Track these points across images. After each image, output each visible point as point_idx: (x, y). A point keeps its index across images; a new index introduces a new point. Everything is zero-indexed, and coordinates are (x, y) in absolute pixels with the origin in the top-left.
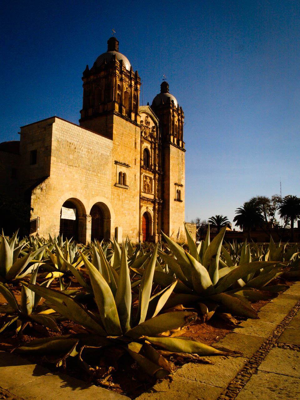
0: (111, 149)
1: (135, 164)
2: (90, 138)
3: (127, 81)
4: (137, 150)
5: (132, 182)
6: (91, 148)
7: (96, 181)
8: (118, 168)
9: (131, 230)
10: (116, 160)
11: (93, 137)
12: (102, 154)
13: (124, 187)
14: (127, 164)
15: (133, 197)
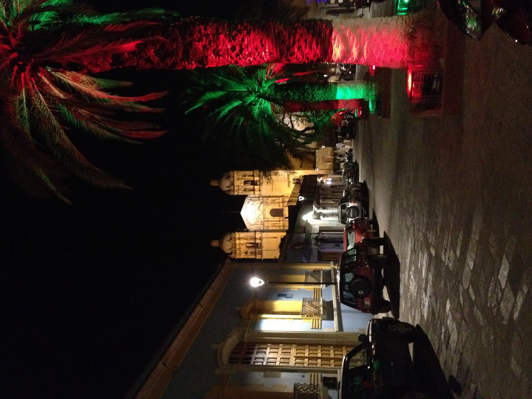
3: (239, 246)
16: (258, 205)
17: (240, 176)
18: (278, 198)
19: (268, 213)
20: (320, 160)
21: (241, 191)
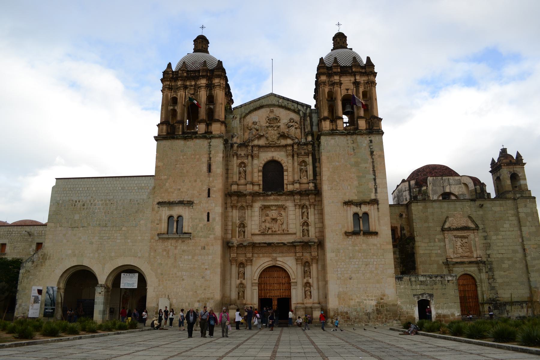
0: (150, 188)
1: (209, 196)
2: (110, 186)
3: (191, 86)
4: (212, 174)
6: (112, 197)
7: (120, 238)
8: (164, 212)
9: (199, 301)
10: (161, 200)
11: (115, 182)
12: (131, 200)
13: (177, 236)
14: (188, 201)
15: (204, 248)
18: (311, 178)
19: (273, 157)
20: (423, 287)
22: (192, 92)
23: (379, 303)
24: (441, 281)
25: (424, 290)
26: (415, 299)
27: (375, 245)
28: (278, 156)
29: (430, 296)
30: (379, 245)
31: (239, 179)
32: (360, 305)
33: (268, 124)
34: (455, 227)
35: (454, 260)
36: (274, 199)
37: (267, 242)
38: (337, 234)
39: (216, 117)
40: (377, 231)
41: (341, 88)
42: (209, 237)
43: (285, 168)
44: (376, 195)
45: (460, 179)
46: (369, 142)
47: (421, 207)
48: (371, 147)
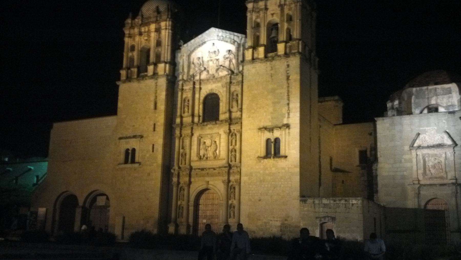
1: (154, 130)
3: (145, 32)
4: (157, 111)
5: (148, 155)
9: (143, 219)
10: (121, 136)
14: (139, 136)
15: (149, 174)
16: (227, 64)
17: (290, 9)
18: (239, 107)
20: (326, 210)
21: (254, 18)
22: (146, 38)
23: (283, 224)
24: (345, 204)
25: (327, 213)
26: (317, 221)
27: (283, 168)
28: (216, 88)
29: (332, 219)
30: (287, 169)
31: (184, 113)
32: (266, 226)
33: (209, 59)
34: (426, 145)
35: (422, 182)
36: (209, 128)
37: (201, 168)
38: (251, 159)
39: (162, 59)
40: (287, 155)
41: (267, 13)
42: (153, 165)
43: (221, 99)
44: (288, 120)
45: (450, 88)
46: (286, 67)
47: (387, 125)
48: (288, 72)
